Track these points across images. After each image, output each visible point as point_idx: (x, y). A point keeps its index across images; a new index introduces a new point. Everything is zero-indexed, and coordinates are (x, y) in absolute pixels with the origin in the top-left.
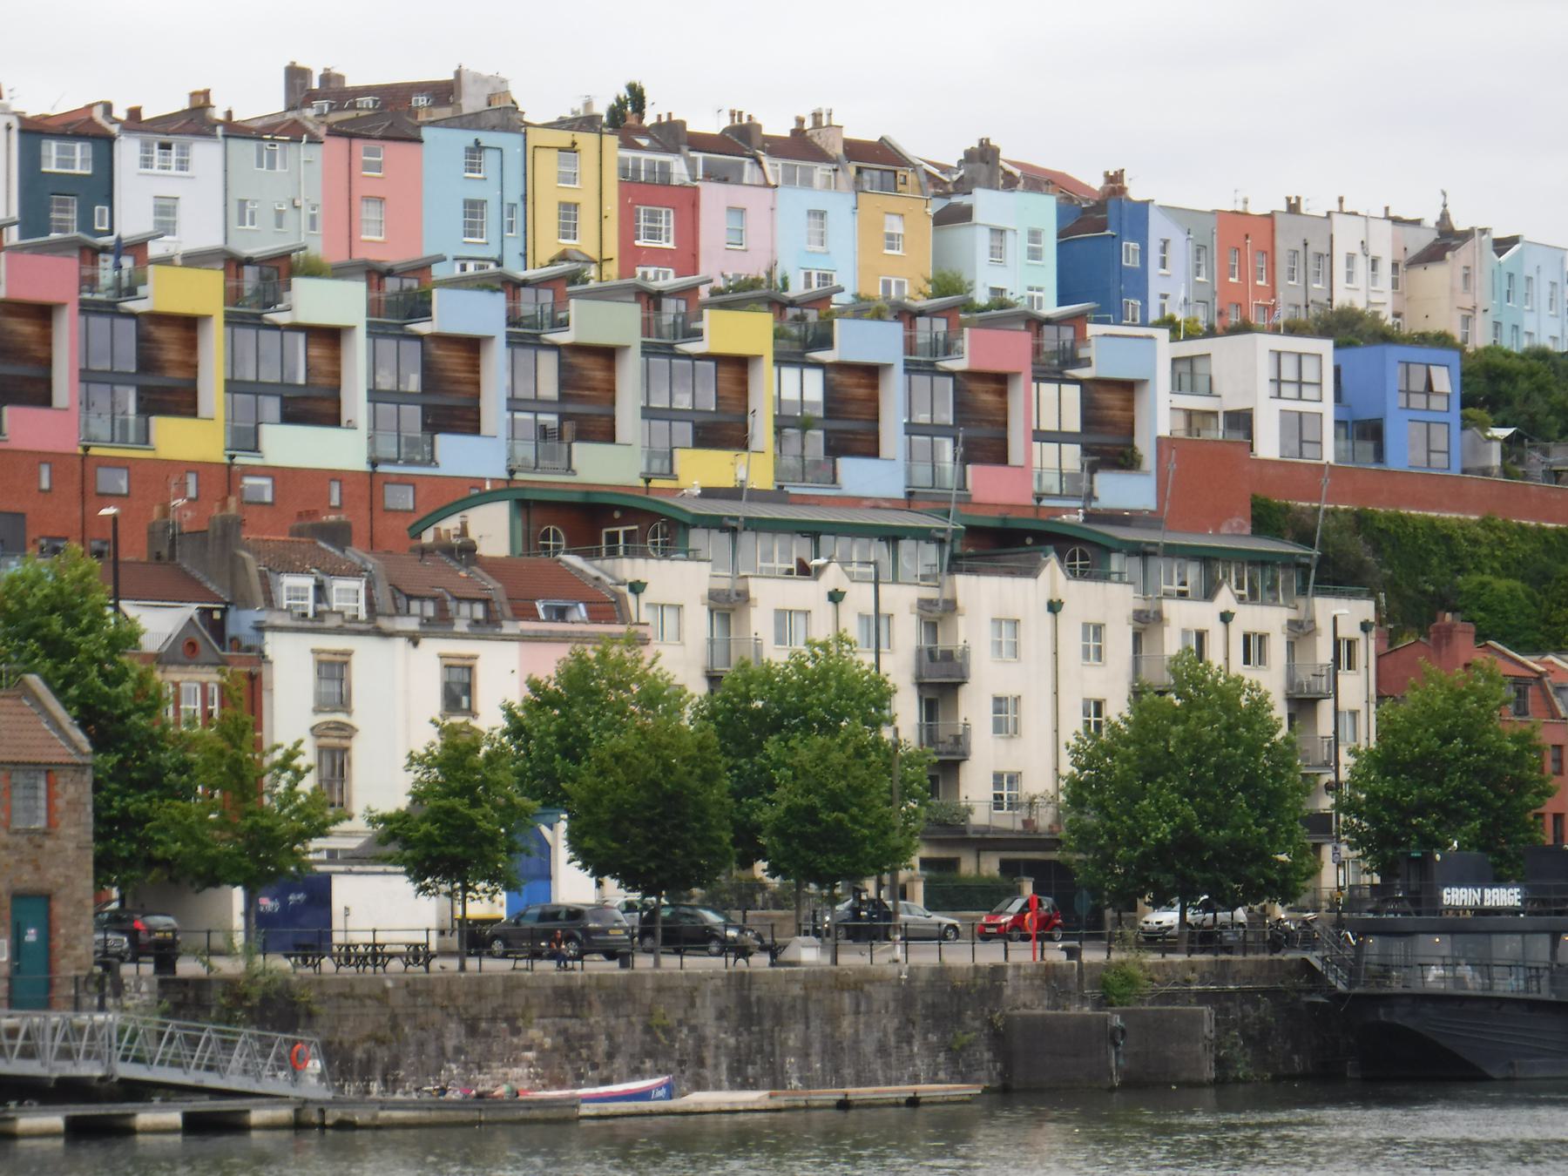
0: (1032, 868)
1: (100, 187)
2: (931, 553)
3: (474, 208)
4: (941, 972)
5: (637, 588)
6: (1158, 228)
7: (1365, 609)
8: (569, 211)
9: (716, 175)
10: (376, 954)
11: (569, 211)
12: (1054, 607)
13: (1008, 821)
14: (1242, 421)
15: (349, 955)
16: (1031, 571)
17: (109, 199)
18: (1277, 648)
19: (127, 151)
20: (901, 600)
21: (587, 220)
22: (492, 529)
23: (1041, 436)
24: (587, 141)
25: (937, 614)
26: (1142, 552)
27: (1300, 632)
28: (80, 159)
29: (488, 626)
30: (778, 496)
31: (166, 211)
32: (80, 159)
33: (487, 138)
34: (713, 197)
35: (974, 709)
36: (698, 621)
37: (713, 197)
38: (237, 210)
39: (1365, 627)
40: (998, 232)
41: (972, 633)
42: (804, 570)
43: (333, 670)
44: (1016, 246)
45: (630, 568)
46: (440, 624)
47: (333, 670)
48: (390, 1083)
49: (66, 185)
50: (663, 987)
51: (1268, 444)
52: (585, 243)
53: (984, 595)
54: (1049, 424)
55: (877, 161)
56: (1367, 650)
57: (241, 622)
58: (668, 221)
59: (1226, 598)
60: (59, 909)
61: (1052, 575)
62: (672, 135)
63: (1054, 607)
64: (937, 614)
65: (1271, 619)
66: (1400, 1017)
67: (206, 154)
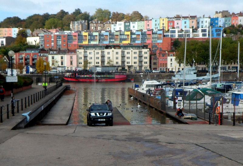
3: (156, 24)
5: (78, 51)
8: (163, 24)
11: (163, 24)
17: (130, 26)
21: (165, 24)
31: (134, 27)
36: (83, 53)
38: (138, 26)
39: (148, 51)
40: (202, 21)
41: (106, 54)
44: (204, 22)
49: (127, 26)
53: (106, 51)
61: (113, 49)
63: (113, 51)
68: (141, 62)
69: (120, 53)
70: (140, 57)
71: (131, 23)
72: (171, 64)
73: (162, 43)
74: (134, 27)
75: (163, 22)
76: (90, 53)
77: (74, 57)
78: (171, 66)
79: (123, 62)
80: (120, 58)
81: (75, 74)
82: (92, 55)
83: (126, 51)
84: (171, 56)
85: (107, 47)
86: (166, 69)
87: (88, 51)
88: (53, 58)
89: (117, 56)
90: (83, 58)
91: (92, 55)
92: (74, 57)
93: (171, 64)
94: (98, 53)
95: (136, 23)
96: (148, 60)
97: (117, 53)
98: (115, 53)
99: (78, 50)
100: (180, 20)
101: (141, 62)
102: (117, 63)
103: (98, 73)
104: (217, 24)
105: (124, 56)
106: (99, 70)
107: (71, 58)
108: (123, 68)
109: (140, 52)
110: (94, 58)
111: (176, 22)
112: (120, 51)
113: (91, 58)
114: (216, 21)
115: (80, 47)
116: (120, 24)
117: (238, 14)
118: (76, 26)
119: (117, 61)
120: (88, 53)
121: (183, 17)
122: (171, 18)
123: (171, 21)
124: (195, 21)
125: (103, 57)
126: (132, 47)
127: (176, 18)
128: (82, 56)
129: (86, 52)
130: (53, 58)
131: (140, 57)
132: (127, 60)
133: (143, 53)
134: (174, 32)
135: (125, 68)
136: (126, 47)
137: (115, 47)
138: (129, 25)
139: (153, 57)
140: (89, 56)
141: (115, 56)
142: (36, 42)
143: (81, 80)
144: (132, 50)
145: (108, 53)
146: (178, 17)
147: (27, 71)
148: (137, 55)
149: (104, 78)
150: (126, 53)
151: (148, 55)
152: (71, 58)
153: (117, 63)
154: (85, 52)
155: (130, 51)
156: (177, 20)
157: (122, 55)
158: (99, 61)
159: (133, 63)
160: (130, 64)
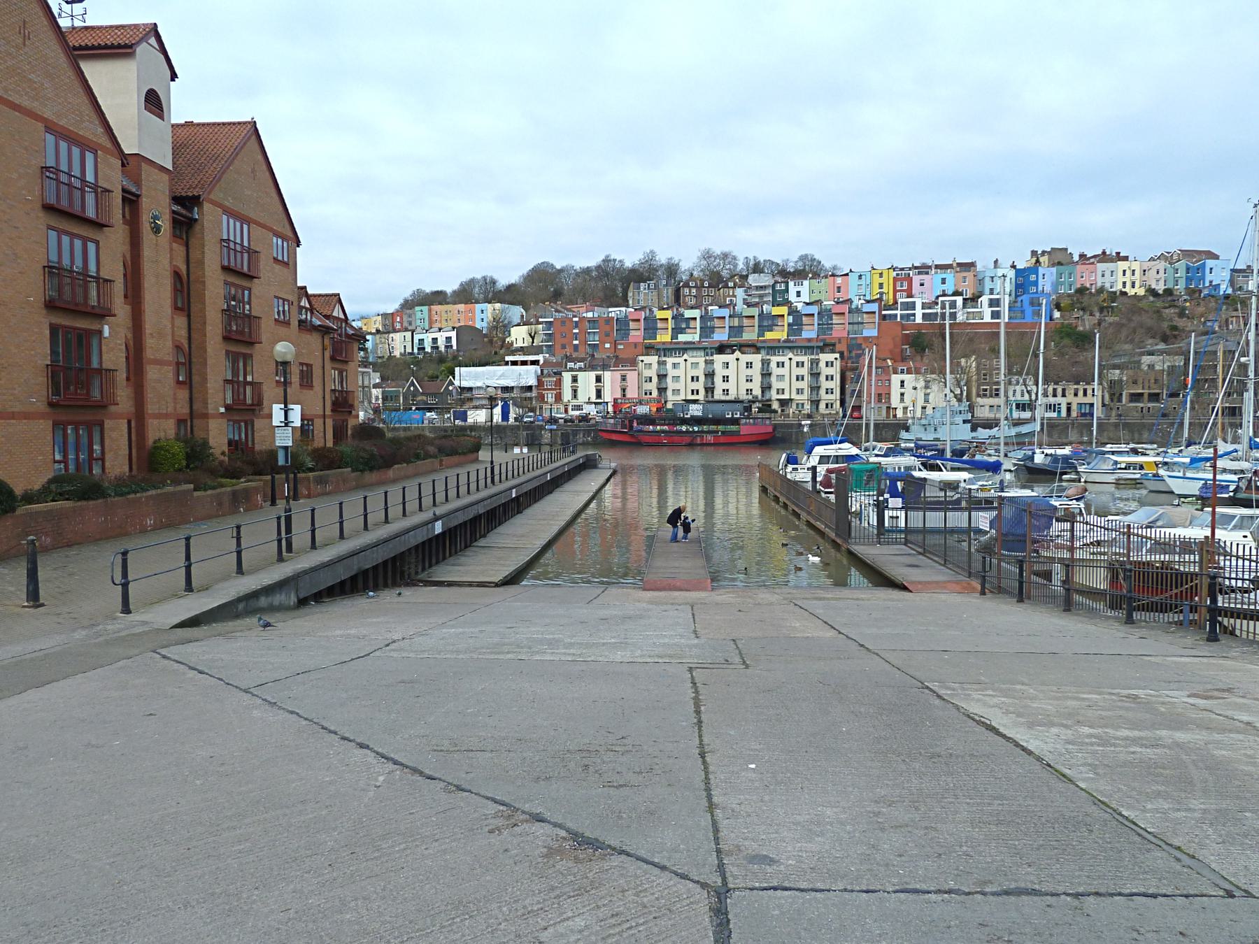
8: (881, 286)
11: (881, 286)
30: (786, 341)
31: (798, 294)
36: (655, 366)
41: (718, 367)
49: (781, 292)
53: (719, 359)
58: (905, 284)
61: (737, 354)
68: (815, 389)
69: (757, 366)
70: (815, 375)
71: (791, 284)
72: (902, 394)
73: (877, 337)
74: (798, 294)
75: (881, 280)
76: (675, 366)
77: (632, 376)
78: (902, 400)
79: (766, 388)
80: (757, 379)
81: (631, 422)
82: (680, 372)
83: (774, 360)
84: (902, 372)
85: (722, 349)
86: (888, 408)
87: (670, 361)
88: (575, 379)
89: (749, 372)
90: (655, 379)
91: (680, 372)
92: (632, 376)
93: (902, 394)
94: (695, 365)
95: (806, 283)
96: (835, 384)
97: (749, 365)
98: (743, 365)
99: (641, 358)
100: (927, 273)
101: (815, 389)
102: (749, 391)
103: (696, 421)
104: (1036, 283)
105: (770, 374)
106: (695, 410)
107: (624, 378)
108: (766, 407)
109: (815, 363)
110: (683, 379)
111: (916, 280)
112: (756, 359)
113: (676, 378)
114: (1033, 278)
115: (649, 349)
117: (1095, 257)
118: (642, 294)
119: (749, 386)
120: (669, 366)
121: (937, 267)
122: (902, 269)
123: (903, 278)
124: (969, 275)
125: (710, 375)
126: (790, 348)
127: (916, 268)
128: (652, 373)
129: (664, 363)
130: (575, 379)
131: (815, 375)
132: (776, 384)
133: (822, 364)
134: (912, 306)
135: (770, 406)
136: (774, 348)
137: (744, 347)
138: (787, 290)
139: (850, 375)
140: (671, 372)
141: (745, 372)
142: (533, 338)
143: (647, 439)
144: (790, 355)
146: (924, 269)
147: (505, 415)
148: (804, 371)
149: (709, 432)
150: (773, 365)
151: (835, 371)
152: (624, 378)
153: (749, 391)
154: (662, 364)
155: (785, 359)
156: (919, 273)
157: (763, 369)
158: (700, 385)
159: (794, 391)
160: (786, 396)
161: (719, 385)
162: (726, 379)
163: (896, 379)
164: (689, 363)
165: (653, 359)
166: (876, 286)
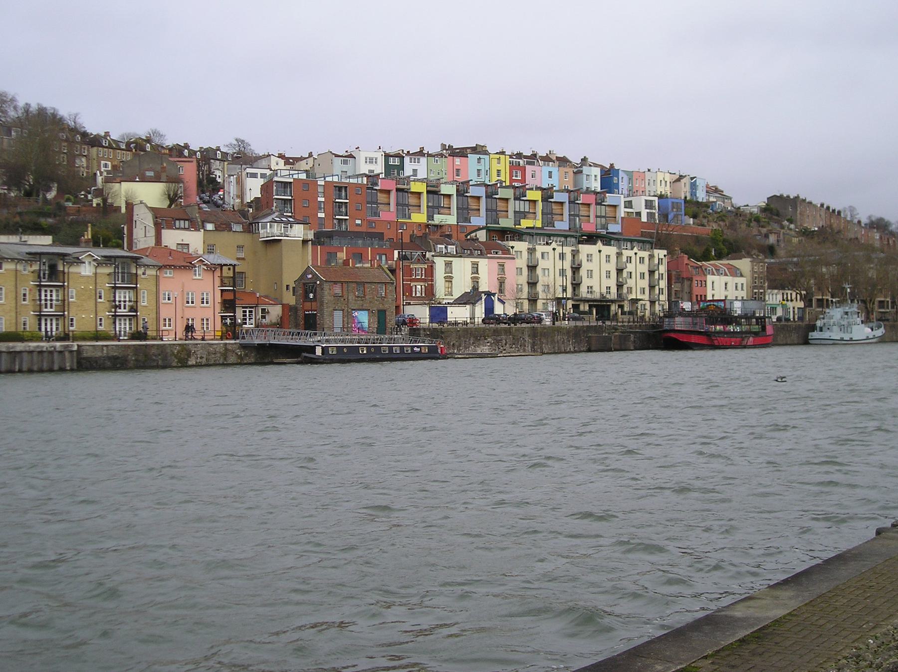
0: (595, 306)
1: (401, 167)
2: (573, 239)
3: (479, 170)
4: (576, 326)
5: (512, 247)
6: (621, 174)
7: (665, 252)
8: (499, 171)
9: (529, 163)
10: (456, 323)
11: (499, 171)
12: (600, 251)
13: (589, 296)
14: (639, 214)
15: (451, 324)
16: (595, 244)
18: (646, 260)
19: (407, 160)
20: (568, 250)
22: (482, 236)
23: (597, 217)
24: (502, 157)
25: (575, 254)
26: (618, 240)
27: (651, 257)
28: (397, 162)
29: (482, 255)
30: (542, 228)
31: (415, 171)
32: (397, 162)
33: (482, 156)
34: (529, 168)
35: (583, 272)
36: (525, 254)
37: (529, 168)
38: (429, 171)
41: (582, 257)
42: (547, 244)
43: (448, 265)
45: (511, 243)
46: (471, 255)
47: (448, 265)
48: (459, 350)
50: (517, 330)
51: (644, 219)
52: (502, 178)
53: (585, 249)
54: (599, 214)
55: (563, 161)
56: (665, 261)
57: (428, 255)
58: (519, 174)
59: (635, 250)
60: (387, 313)
62: (519, 155)
63: (600, 251)
64: (575, 254)
65: (645, 254)
66: (672, 335)
67: (423, 160)
91: (594, 266)
112: (612, 250)
116: (371, 159)
128: (522, 262)
145: (589, 257)
146: (533, 158)
161: (586, 282)
162: (590, 273)
163: (710, 278)
164: (603, 254)
165: (521, 246)
166: (494, 173)
